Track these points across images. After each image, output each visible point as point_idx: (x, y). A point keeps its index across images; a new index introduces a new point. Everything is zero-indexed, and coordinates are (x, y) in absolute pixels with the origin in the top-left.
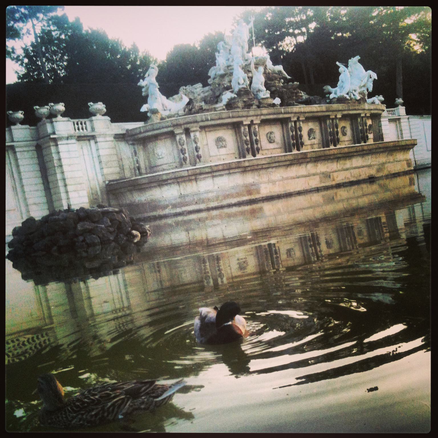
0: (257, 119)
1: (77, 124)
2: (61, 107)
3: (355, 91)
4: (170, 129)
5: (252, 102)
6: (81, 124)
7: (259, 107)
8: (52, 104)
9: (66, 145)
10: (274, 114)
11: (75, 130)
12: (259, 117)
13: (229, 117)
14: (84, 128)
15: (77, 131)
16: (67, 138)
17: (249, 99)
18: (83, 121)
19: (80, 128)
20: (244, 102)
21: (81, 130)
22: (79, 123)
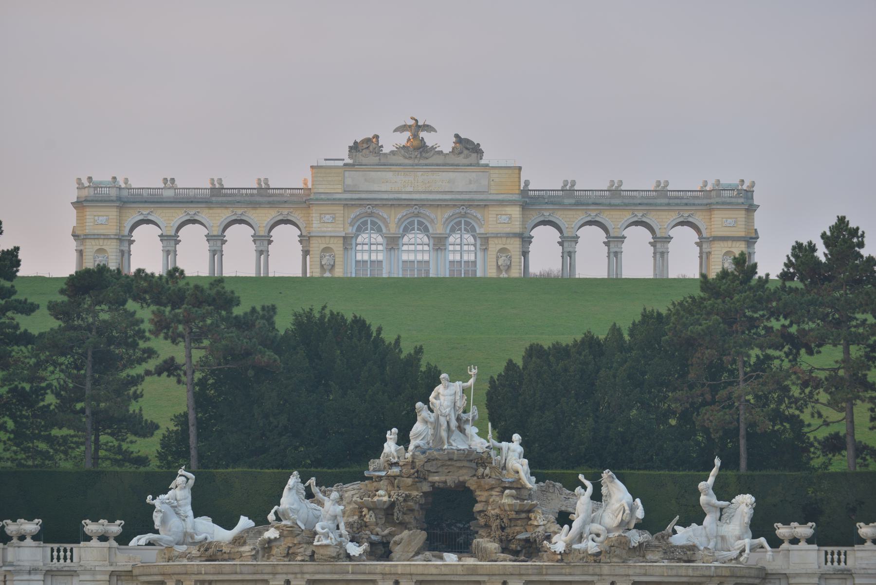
0: (296, 578)
1: (59, 551)
2: (32, 527)
3: (598, 535)
4: (159, 578)
5: (299, 551)
6: (65, 551)
7: (312, 557)
8: (22, 520)
9: (27, 582)
10: (331, 573)
11: (52, 559)
12: (299, 576)
13: (241, 573)
14: (69, 557)
15: (55, 560)
16: (30, 573)
17: (295, 544)
18: (68, 546)
19: (62, 557)
20: (289, 548)
21: (62, 561)
22: (62, 549)
